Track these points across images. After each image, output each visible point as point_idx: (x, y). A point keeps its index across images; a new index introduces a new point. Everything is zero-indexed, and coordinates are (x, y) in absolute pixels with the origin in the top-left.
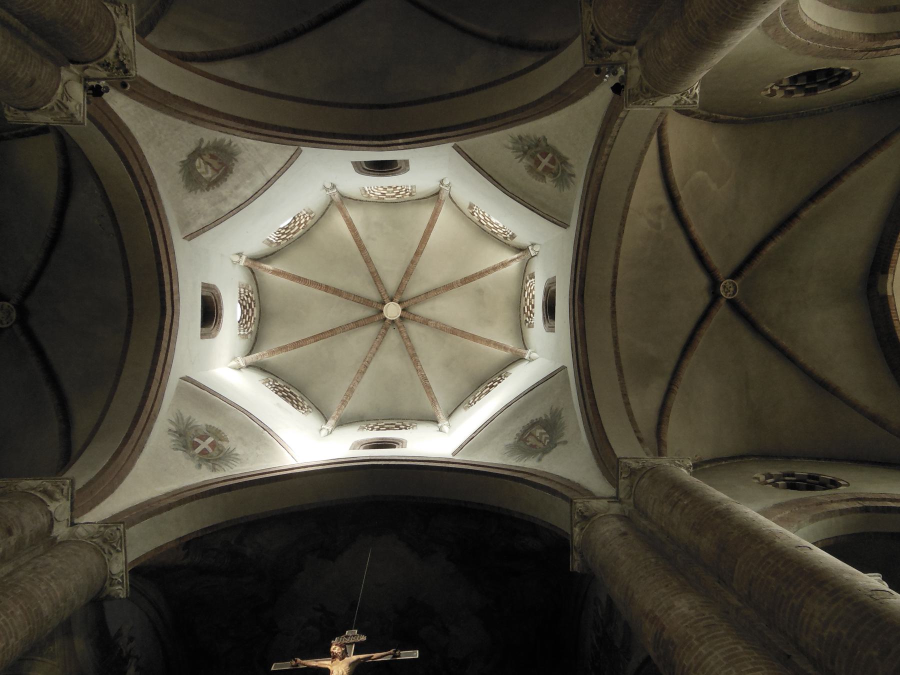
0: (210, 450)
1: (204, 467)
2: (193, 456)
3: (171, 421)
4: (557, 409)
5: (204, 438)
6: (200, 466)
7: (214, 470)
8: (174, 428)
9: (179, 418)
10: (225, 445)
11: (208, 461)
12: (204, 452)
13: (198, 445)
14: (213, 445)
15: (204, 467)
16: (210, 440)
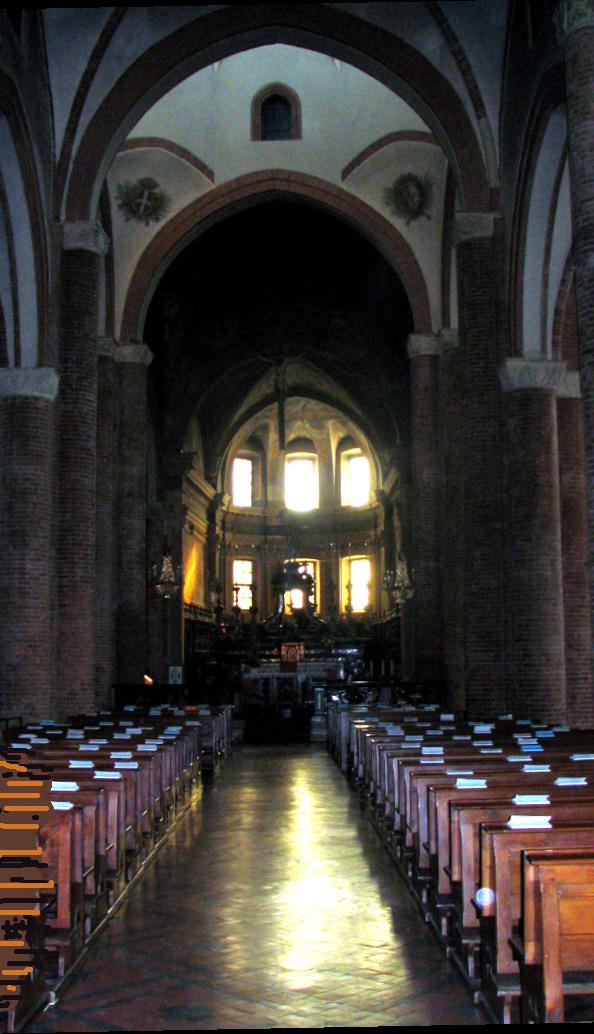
0: (149, 203)
1: (151, 223)
2: (140, 219)
3: (117, 198)
4: (430, 180)
5: (141, 196)
6: (147, 224)
7: (158, 220)
8: (120, 202)
9: (120, 188)
10: (157, 191)
11: (150, 215)
12: (146, 207)
13: (140, 205)
14: (150, 198)
15: (151, 223)
16: (146, 193)
